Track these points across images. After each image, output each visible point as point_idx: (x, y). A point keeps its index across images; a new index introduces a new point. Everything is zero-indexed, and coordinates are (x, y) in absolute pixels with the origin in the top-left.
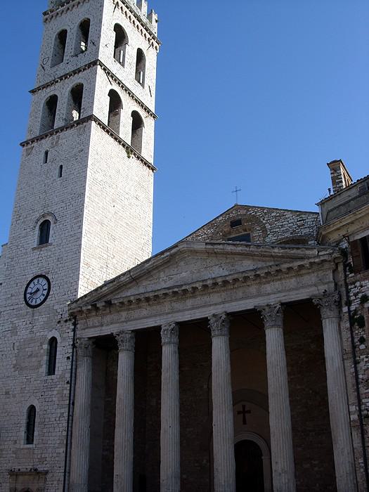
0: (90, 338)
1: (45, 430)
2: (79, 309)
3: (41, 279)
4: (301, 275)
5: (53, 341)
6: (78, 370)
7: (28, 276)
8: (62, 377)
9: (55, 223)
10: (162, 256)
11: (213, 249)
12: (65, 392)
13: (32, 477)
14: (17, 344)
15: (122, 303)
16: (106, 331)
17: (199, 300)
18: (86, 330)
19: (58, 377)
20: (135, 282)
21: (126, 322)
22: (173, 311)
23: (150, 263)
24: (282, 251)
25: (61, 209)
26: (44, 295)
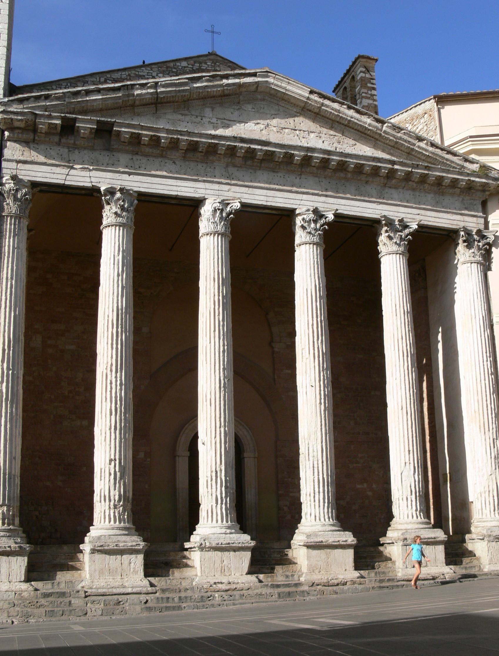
0: (34, 185)
2: (30, 117)
4: (443, 194)
10: (225, 81)
11: (323, 104)
18: (28, 166)
24: (431, 149)
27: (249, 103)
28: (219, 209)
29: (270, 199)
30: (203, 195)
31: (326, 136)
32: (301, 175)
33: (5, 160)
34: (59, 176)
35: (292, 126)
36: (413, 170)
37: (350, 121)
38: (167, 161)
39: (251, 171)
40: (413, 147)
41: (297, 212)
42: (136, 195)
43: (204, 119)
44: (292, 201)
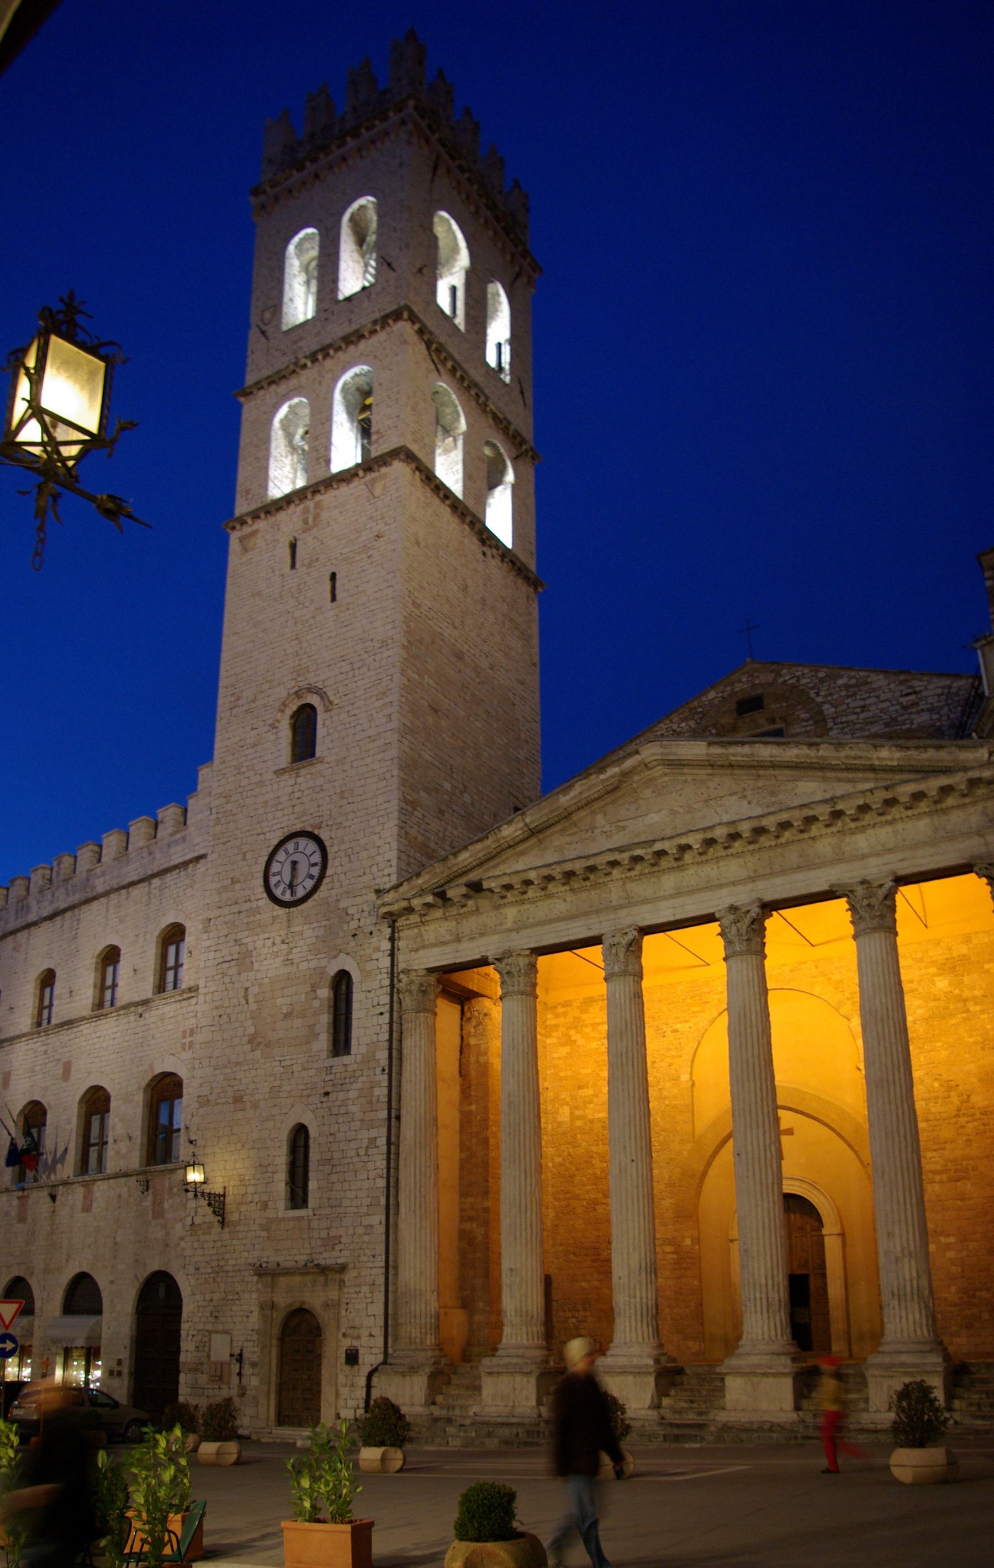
0: (430, 970)
1: (334, 1178)
2: (404, 904)
3: (303, 842)
5: (342, 982)
6: (407, 1043)
7: (268, 836)
8: (369, 1059)
9: (327, 711)
13: (309, 1278)
14: (254, 990)
15: (508, 887)
16: (469, 952)
17: (692, 875)
18: (421, 953)
19: (359, 1058)
20: (533, 840)
22: (629, 902)
25: (341, 677)
26: (311, 877)
42: (528, 952)
43: (596, 831)
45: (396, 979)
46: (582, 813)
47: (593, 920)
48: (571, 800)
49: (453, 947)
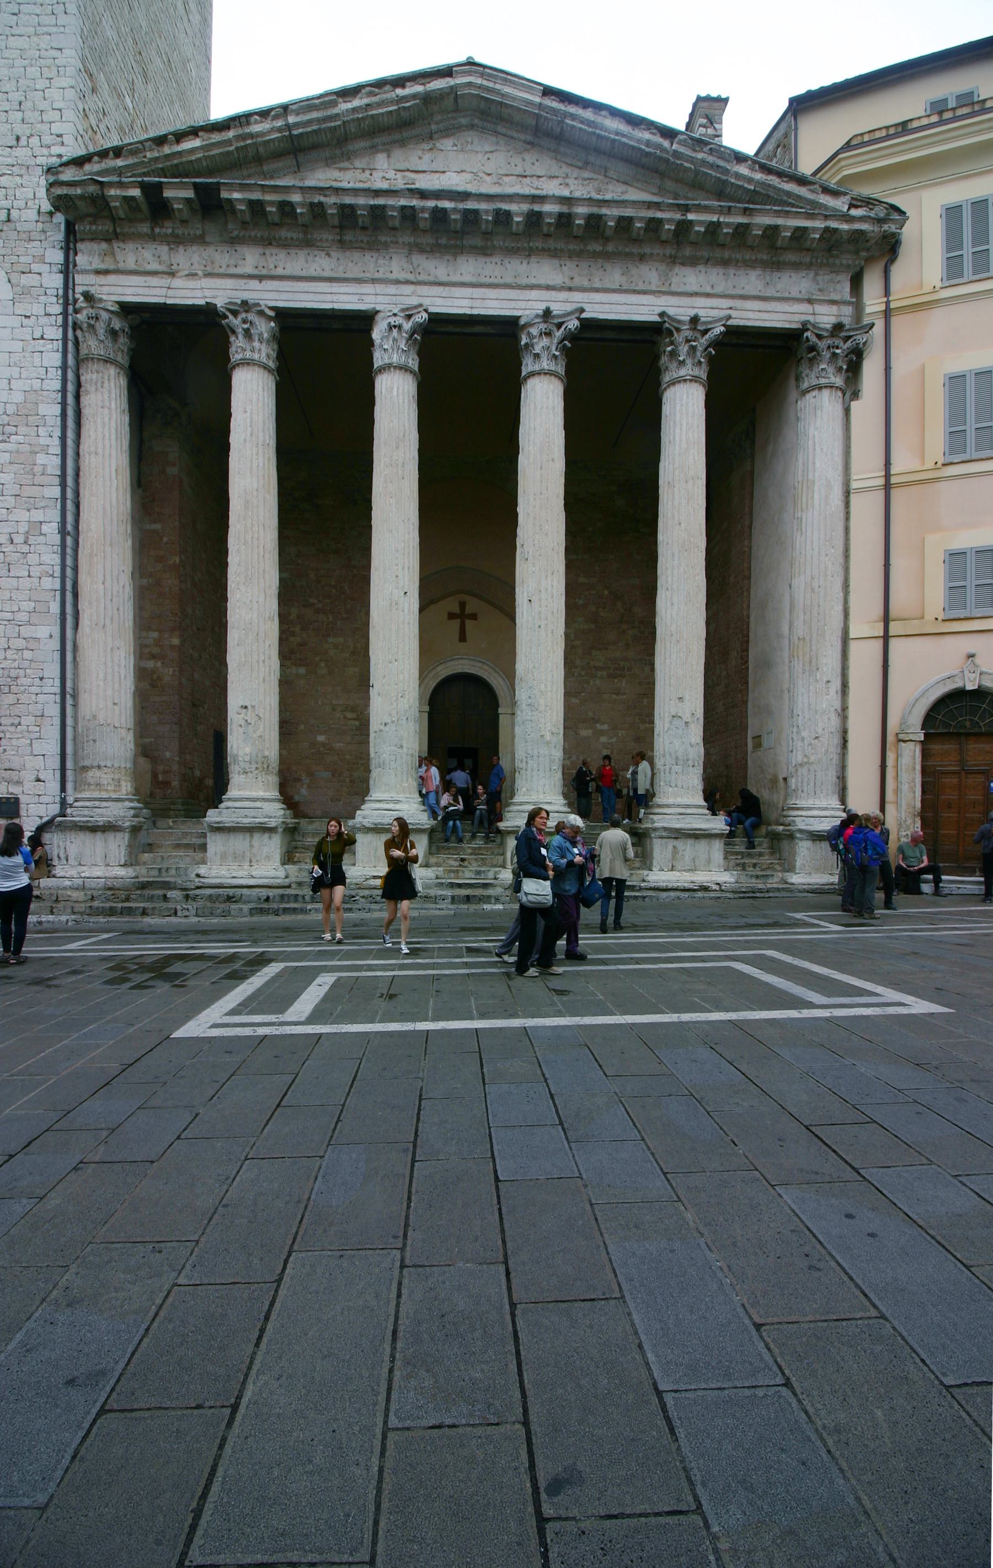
0: (126, 309)
10: (400, 92)
12: (41, 459)
15: (256, 207)
16: (188, 291)
18: (112, 279)
20: (290, 161)
21: (261, 278)
23: (356, 103)
24: (759, 176)
27: (447, 136)
28: (395, 327)
29: (477, 303)
30: (373, 306)
31: (576, 182)
32: (530, 255)
33: (78, 272)
34: (157, 292)
35: (519, 170)
36: (721, 220)
37: (614, 140)
38: (316, 252)
39: (447, 257)
40: (724, 178)
41: (522, 322)
44: (513, 304)
45: (71, 308)
46: (362, 144)
47: (368, 288)
48: (354, 110)
49: (165, 281)
